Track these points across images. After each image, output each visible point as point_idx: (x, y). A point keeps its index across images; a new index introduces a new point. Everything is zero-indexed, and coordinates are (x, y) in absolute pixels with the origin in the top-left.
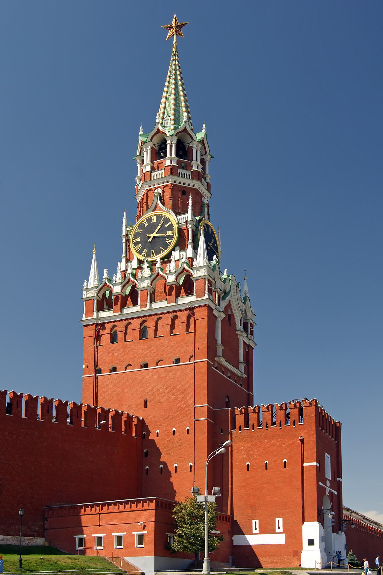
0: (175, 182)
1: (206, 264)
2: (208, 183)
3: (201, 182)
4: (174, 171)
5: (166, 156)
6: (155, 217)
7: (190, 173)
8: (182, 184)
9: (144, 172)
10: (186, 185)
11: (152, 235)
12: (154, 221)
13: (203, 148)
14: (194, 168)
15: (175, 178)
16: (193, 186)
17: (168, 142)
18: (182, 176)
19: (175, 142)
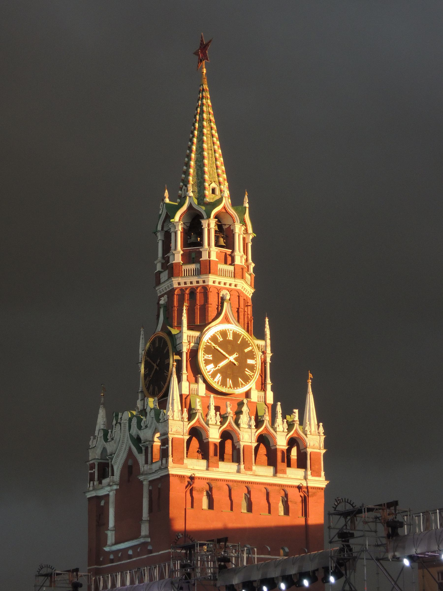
0: (179, 284)
8: (189, 285)
10: (195, 284)
12: (157, 345)
14: (205, 257)
16: (204, 282)
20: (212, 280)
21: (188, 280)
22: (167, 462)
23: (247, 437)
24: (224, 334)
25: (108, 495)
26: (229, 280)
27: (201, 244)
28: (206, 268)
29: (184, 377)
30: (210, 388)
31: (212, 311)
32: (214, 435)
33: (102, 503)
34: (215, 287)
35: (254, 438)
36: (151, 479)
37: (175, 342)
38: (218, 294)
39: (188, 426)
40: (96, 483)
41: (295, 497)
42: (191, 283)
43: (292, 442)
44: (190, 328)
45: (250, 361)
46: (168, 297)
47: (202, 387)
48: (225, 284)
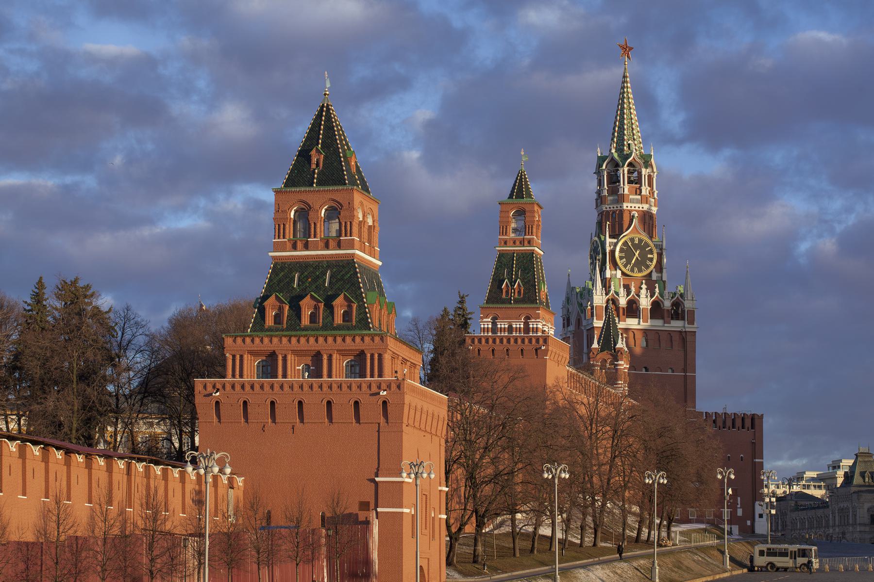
14: (621, 192)
20: (626, 206)
23: (645, 302)
24: (632, 240)
26: (637, 205)
27: (619, 181)
28: (621, 199)
29: (608, 267)
30: (623, 274)
31: (625, 226)
32: (623, 301)
35: (649, 303)
37: (603, 244)
39: (605, 298)
41: (676, 338)
43: (673, 305)
44: (610, 237)
45: (649, 256)
47: (619, 273)
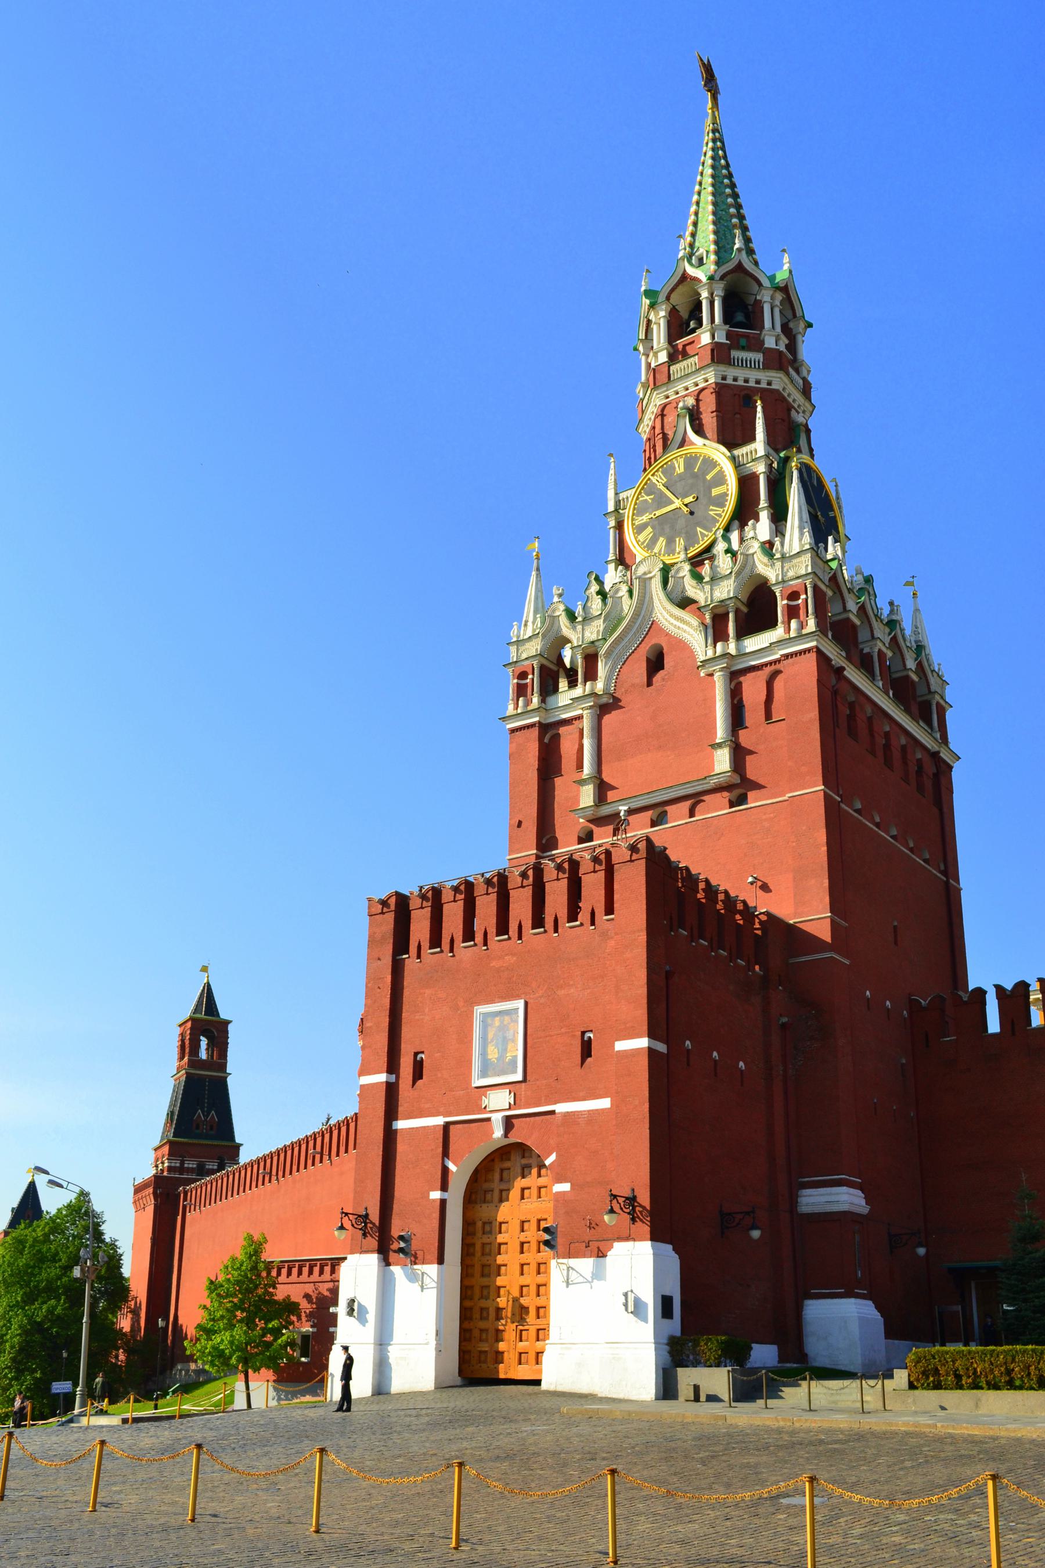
0: (724, 378)
1: (807, 547)
2: (805, 380)
3: (788, 374)
4: (719, 355)
5: (700, 325)
6: (681, 461)
7: (759, 356)
8: (741, 383)
9: (653, 365)
10: (752, 384)
11: (677, 503)
13: (788, 306)
14: (770, 343)
15: (723, 369)
16: (769, 383)
17: (704, 294)
18: (743, 364)
19: (719, 292)
21: (741, 374)
22: (802, 626)
25: (579, 718)
33: (546, 740)
34: (784, 398)
36: (734, 668)
38: (789, 410)
40: (536, 700)
42: (746, 381)
46: (698, 400)
48: (794, 400)
